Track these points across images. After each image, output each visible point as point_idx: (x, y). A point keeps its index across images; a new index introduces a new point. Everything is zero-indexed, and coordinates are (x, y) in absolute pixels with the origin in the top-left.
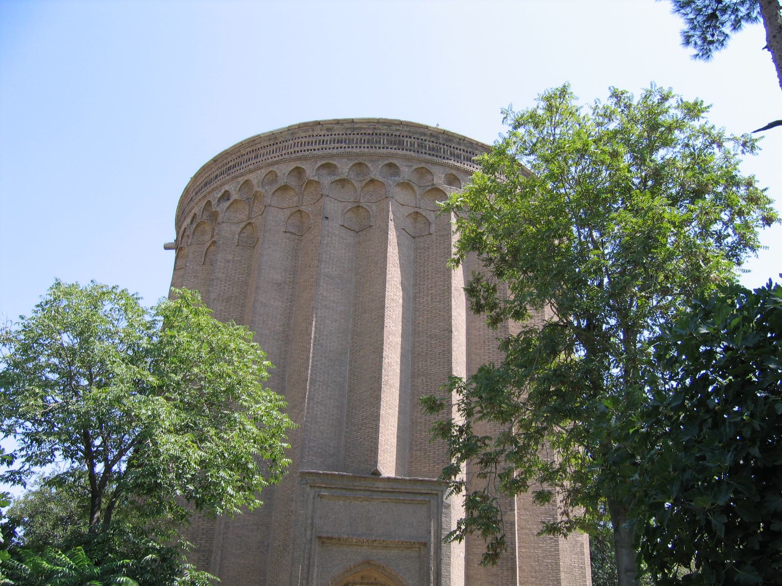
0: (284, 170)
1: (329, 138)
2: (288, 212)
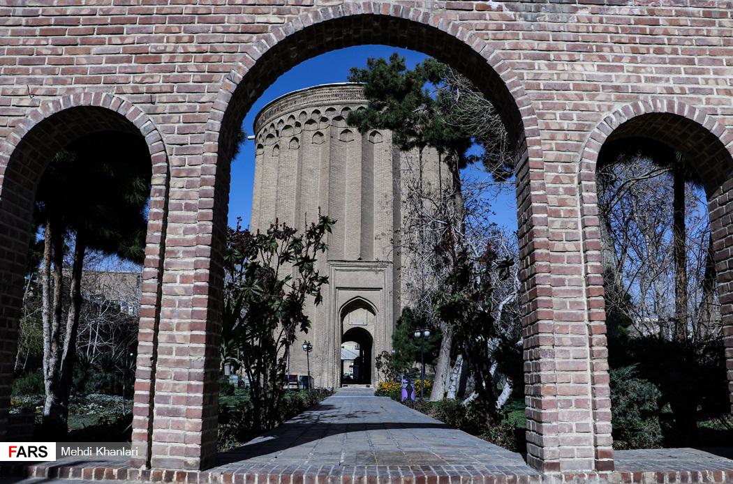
0: (309, 111)
1: (330, 94)
2: (313, 133)
